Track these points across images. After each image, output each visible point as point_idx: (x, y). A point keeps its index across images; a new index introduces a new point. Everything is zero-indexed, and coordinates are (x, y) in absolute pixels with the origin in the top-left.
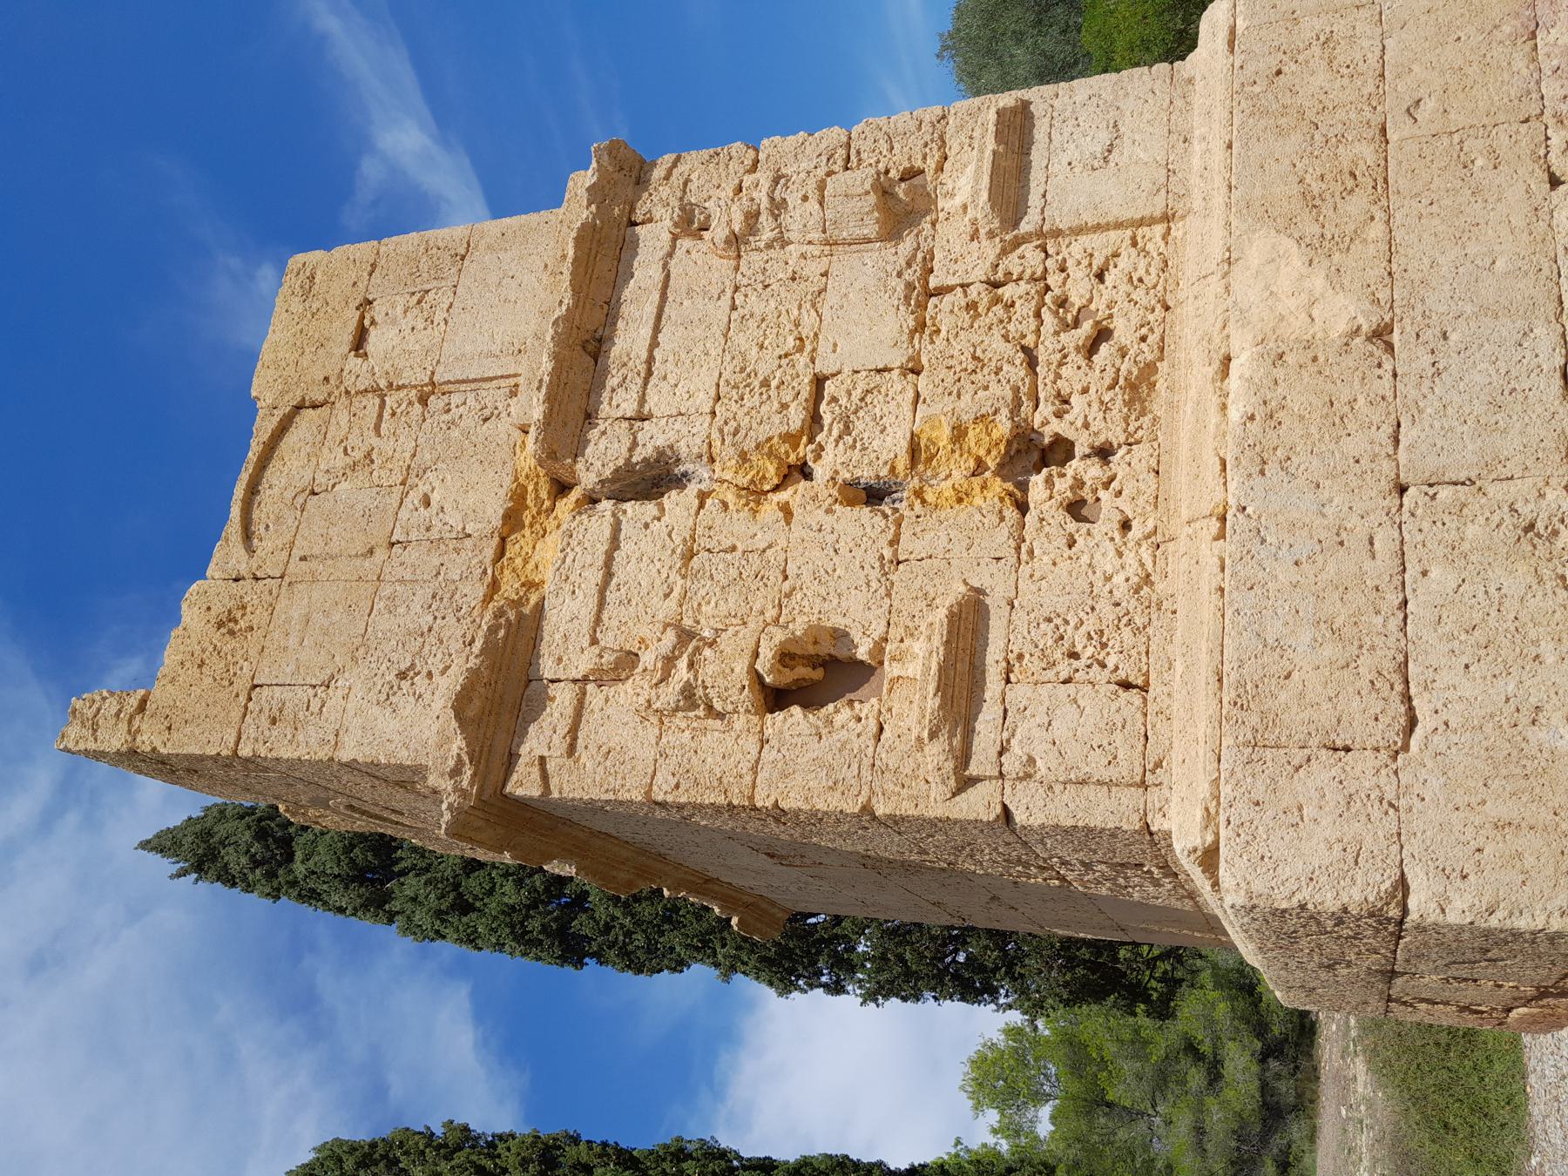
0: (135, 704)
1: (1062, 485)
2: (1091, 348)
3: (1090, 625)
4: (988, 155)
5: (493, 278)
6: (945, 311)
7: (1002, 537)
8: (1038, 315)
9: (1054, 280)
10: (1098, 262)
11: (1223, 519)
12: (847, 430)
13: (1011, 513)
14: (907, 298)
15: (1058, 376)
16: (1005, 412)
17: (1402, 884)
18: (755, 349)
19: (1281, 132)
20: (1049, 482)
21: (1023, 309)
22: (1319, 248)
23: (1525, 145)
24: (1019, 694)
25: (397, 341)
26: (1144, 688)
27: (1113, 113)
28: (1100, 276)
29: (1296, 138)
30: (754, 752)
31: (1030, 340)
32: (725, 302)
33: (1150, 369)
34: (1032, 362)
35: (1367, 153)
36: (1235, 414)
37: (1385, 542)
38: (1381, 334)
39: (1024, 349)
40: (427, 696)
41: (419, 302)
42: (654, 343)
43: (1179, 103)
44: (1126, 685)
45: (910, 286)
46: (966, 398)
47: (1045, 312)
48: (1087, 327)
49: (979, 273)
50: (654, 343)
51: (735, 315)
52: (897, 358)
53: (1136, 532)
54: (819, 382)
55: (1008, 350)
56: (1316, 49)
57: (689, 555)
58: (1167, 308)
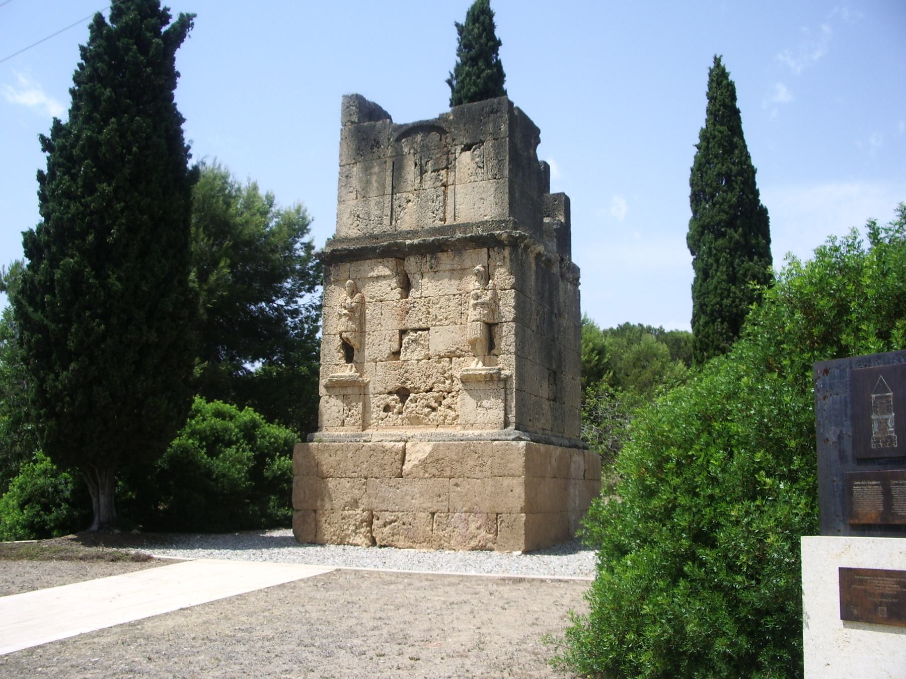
1: (393, 403)
2: (428, 406)
3: (355, 413)
4: (480, 372)
5: (483, 196)
6: (445, 362)
7: (381, 389)
9: (450, 395)
10: (453, 406)
14: (450, 352)
15: (421, 399)
16: (412, 385)
18: (438, 306)
19: (457, 454)
22: (424, 463)
23: (441, 508)
25: (465, 164)
27: (494, 407)
28: (449, 407)
29: (455, 457)
30: (332, 333)
32: (456, 292)
33: (420, 423)
35: (448, 473)
37: (353, 475)
40: (352, 227)
41: (480, 167)
43: (495, 426)
44: (343, 422)
45: (454, 352)
46: (418, 374)
48: (434, 405)
49: (454, 373)
55: (430, 384)
56: (481, 462)
58: (438, 426)
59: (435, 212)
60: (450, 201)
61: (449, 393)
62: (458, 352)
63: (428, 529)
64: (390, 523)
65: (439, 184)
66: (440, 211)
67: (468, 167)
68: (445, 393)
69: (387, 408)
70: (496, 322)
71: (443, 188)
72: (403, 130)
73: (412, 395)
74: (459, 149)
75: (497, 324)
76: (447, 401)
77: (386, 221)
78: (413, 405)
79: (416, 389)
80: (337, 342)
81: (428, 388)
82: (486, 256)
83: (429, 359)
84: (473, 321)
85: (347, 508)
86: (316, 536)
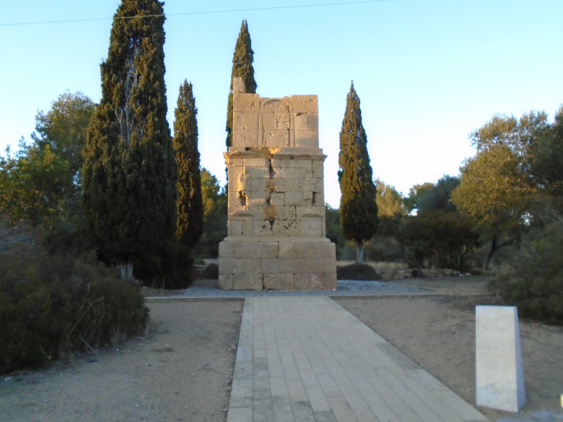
0: (240, 91)
2: (285, 227)
8: (291, 220)
9: (295, 222)
10: (297, 227)
11: (260, 242)
12: (276, 197)
13: (264, 219)
17: (221, 257)
20: (268, 223)
21: (291, 218)
24: (241, 222)
26: (242, 234)
31: (287, 220)
34: (284, 220)
36: (270, 243)
38: (278, 257)
39: (286, 219)
42: (292, 168)
44: (243, 233)
45: (297, 203)
47: (291, 221)
48: (287, 226)
50: (292, 168)
51: (295, 179)
52: (286, 203)
53: (261, 233)
54: (284, 192)
57: (260, 178)
59: (285, 141)
60: (292, 137)
61: (294, 221)
62: (298, 204)
63: (292, 281)
64: (273, 278)
65: (286, 129)
66: (287, 141)
67: (300, 123)
68: (293, 221)
69: (264, 227)
70: (316, 192)
71: (288, 131)
72: (268, 100)
73: (276, 222)
74: (295, 115)
75: (316, 193)
76: (293, 225)
77: (260, 142)
78: (278, 226)
79: (278, 218)
80: (238, 195)
81: (285, 219)
82: (311, 164)
83: (284, 206)
84: (308, 191)
85: (250, 273)
86: (233, 286)
